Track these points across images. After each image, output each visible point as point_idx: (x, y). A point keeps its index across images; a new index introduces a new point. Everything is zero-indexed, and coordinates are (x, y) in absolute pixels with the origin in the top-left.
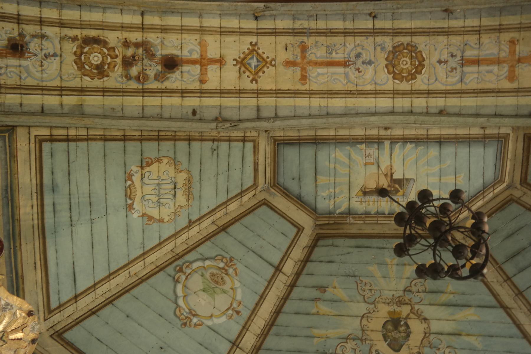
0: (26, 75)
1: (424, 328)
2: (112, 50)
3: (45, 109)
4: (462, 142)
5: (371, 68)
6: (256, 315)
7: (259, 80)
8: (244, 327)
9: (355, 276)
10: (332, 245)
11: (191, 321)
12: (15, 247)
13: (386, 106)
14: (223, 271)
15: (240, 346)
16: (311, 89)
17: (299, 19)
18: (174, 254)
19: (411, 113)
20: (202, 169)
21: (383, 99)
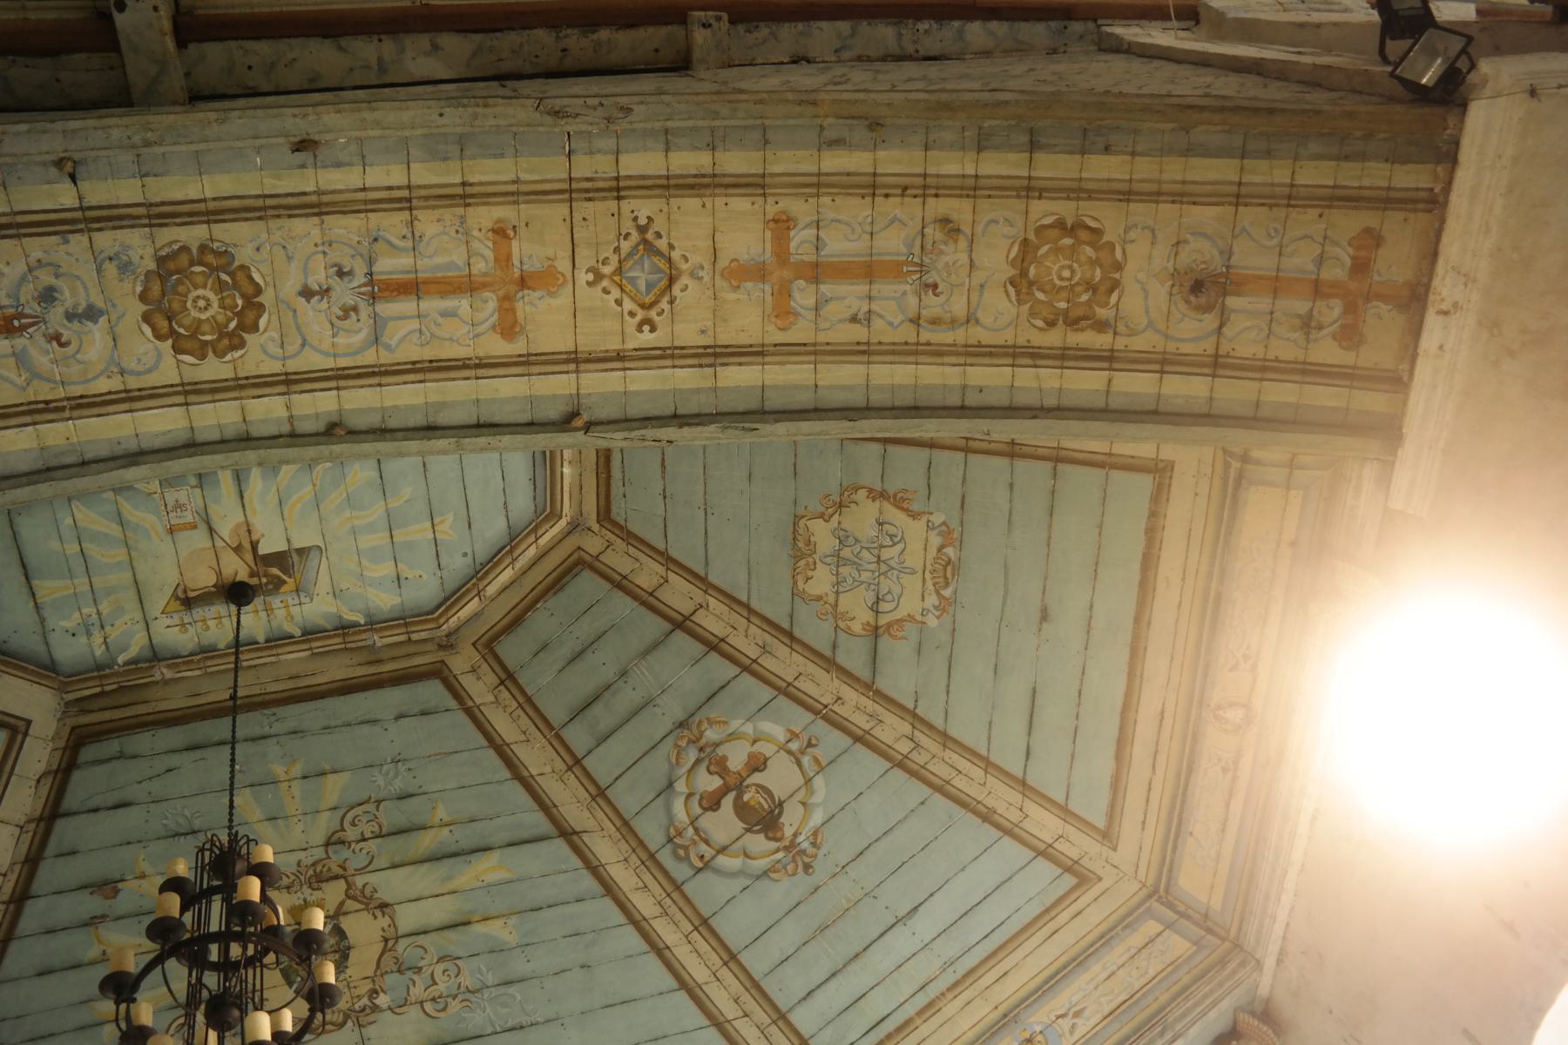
1: (383, 930)
5: (97, 333)
10: (121, 756)
13: (168, 428)
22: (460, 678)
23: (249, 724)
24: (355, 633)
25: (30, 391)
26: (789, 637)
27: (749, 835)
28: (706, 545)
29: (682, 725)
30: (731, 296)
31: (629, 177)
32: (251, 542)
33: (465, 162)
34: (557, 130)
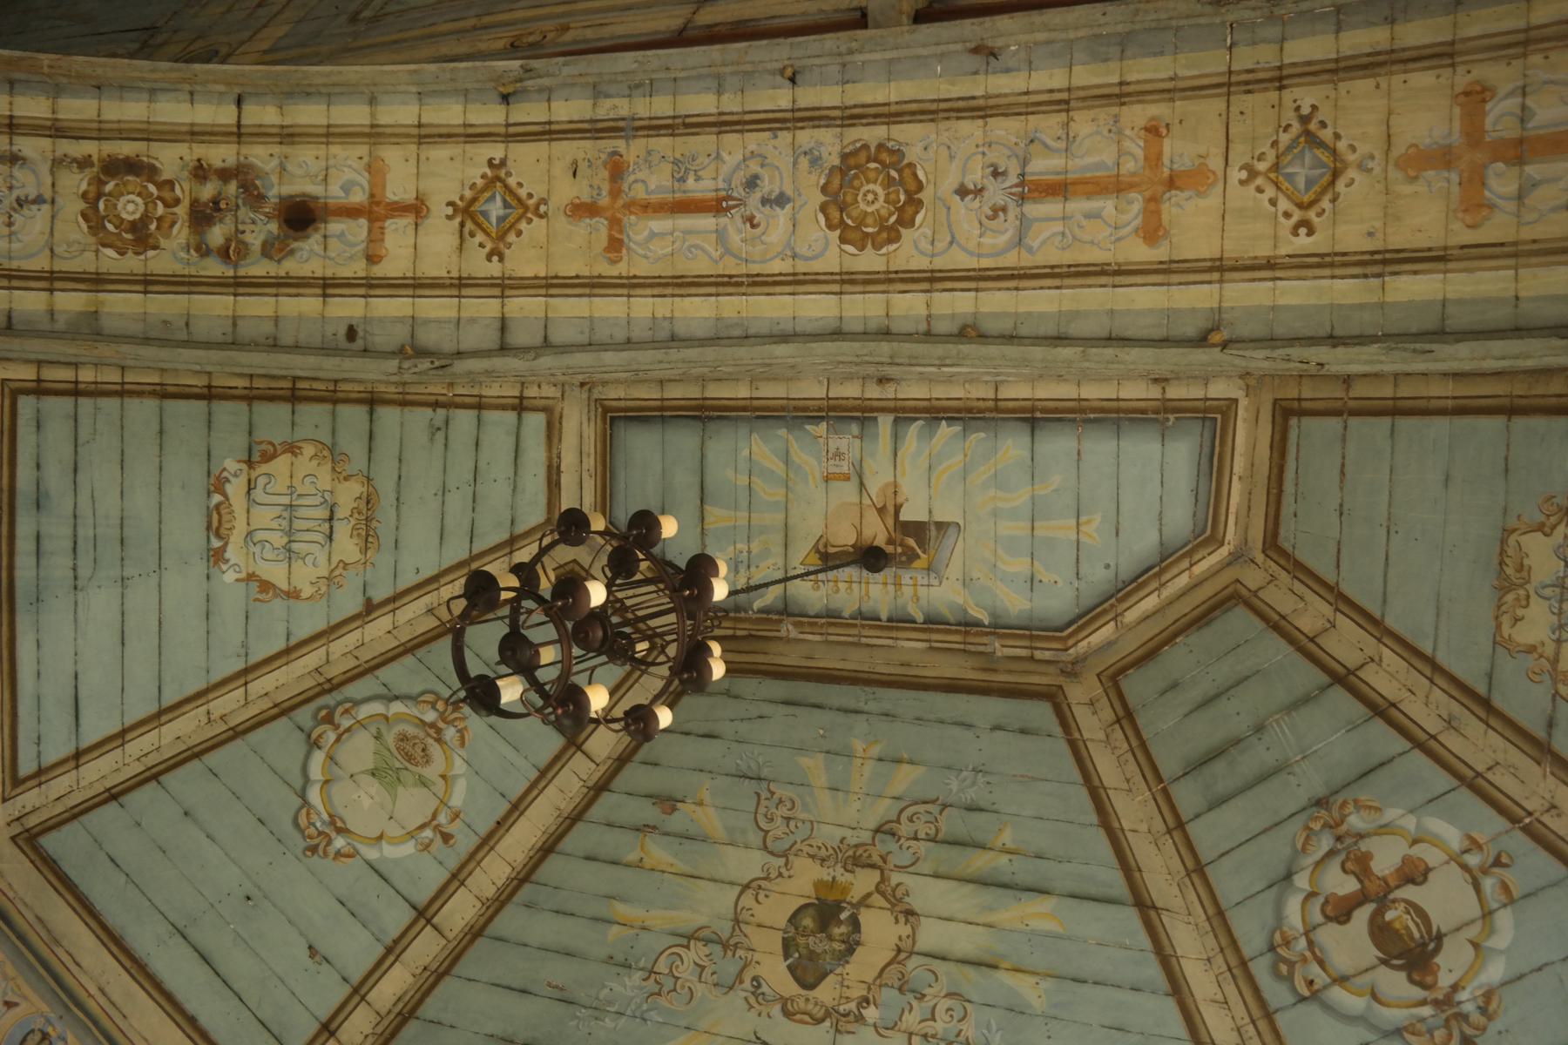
1: (900, 938)
2: (167, 187)
3: (14, 321)
4: (1096, 420)
5: (782, 215)
6: (492, 848)
8: (454, 876)
9: (760, 779)
11: (330, 842)
14: (432, 732)
15: (435, 920)
17: (608, 96)
18: (322, 680)
19: (885, 334)
20: (403, 474)
21: (813, 296)
24: (977, 634)
25: (721, 265)
26: (1484, 706)
27: (1383, 969)
28: (1385, 575)
29: (1320, 803)
30: (1407, 189)
31: (1294, 65)
33: (1125, 62)
34: (1218, 20)
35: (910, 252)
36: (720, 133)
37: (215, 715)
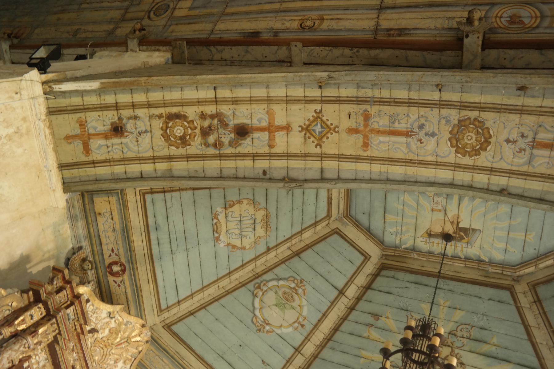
0: (127, 150)
2: (191, 123)
3: (143, 174)
5: (433, 141)
6: (318, 329)
7: (323, 145)
8: (306, 338)
10: (393, 277)
11: (264, 328)
12: (133, 268)
13: (446, 177)
14: (294, 290)
15: (301, 352)
16: (372, 156)
17: (363, 88)
18: (254, 274)
20: (278, 206)
21: (443, 170)
22: (518, 294)
23: (442, 283)
32: (457, 222)
35: (484, 160)
36: (409, 106)
37: (221, 286)
